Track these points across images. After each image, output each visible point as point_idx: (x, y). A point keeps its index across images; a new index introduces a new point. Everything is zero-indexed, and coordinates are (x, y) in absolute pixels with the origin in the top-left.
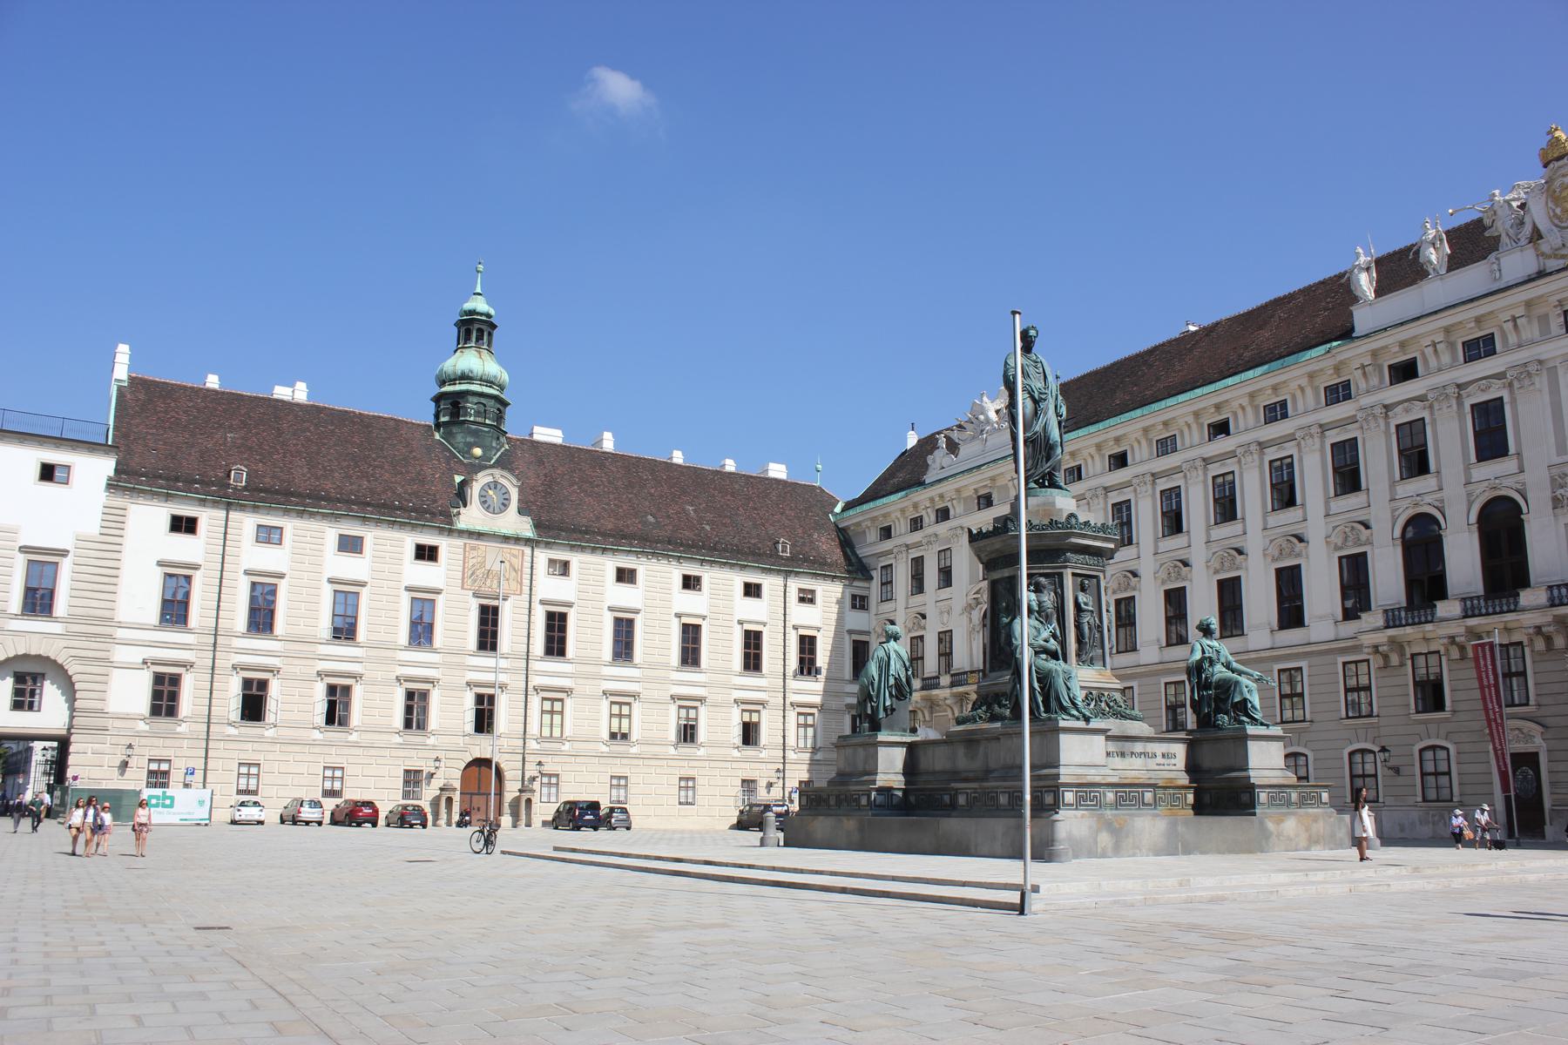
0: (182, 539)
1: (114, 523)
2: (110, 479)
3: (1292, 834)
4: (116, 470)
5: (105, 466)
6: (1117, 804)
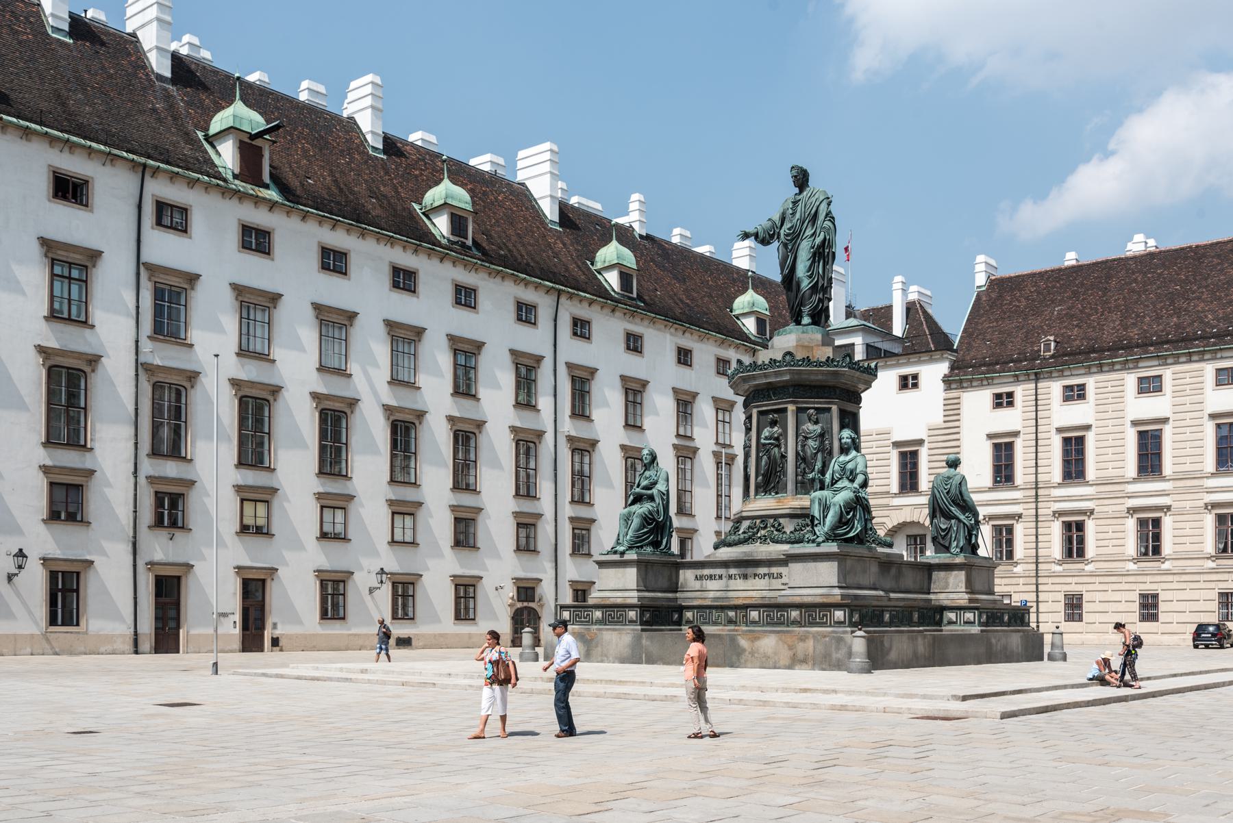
0: (1004, 412)
1: (952, 410)
2: (945, 376)
3: (770, 651)
4: (952, 368)
5: (943, 368)
6: (602, 622)
